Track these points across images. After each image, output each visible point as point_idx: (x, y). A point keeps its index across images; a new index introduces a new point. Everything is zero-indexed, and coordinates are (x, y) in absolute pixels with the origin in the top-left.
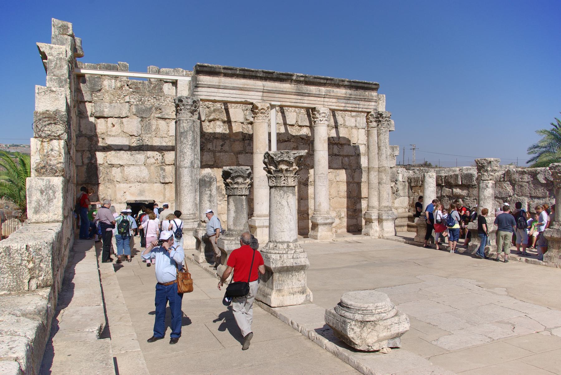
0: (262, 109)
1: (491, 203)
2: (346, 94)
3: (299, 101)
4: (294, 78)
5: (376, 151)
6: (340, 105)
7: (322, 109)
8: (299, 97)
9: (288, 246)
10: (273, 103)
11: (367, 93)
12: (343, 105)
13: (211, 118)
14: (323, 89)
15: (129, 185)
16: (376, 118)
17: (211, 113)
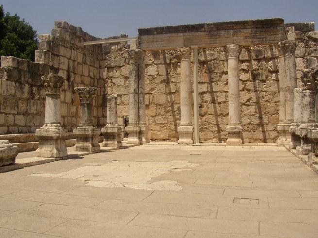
0: (183, 51)
1: (309, 110)
2: (252, 32)
3: (212, 42)
4: (206, 27)
5: (283, 74)
6: (247, 40)
7: (232, 46)
8: (212, 40)
9: (46, 125)
10: (192, 47)
11: (272, 28)
12: (251, 40)
13: (173, 61)
14: (231, 31)
15: (124, 106)
16: (281, 47)
17: (174, 58)
